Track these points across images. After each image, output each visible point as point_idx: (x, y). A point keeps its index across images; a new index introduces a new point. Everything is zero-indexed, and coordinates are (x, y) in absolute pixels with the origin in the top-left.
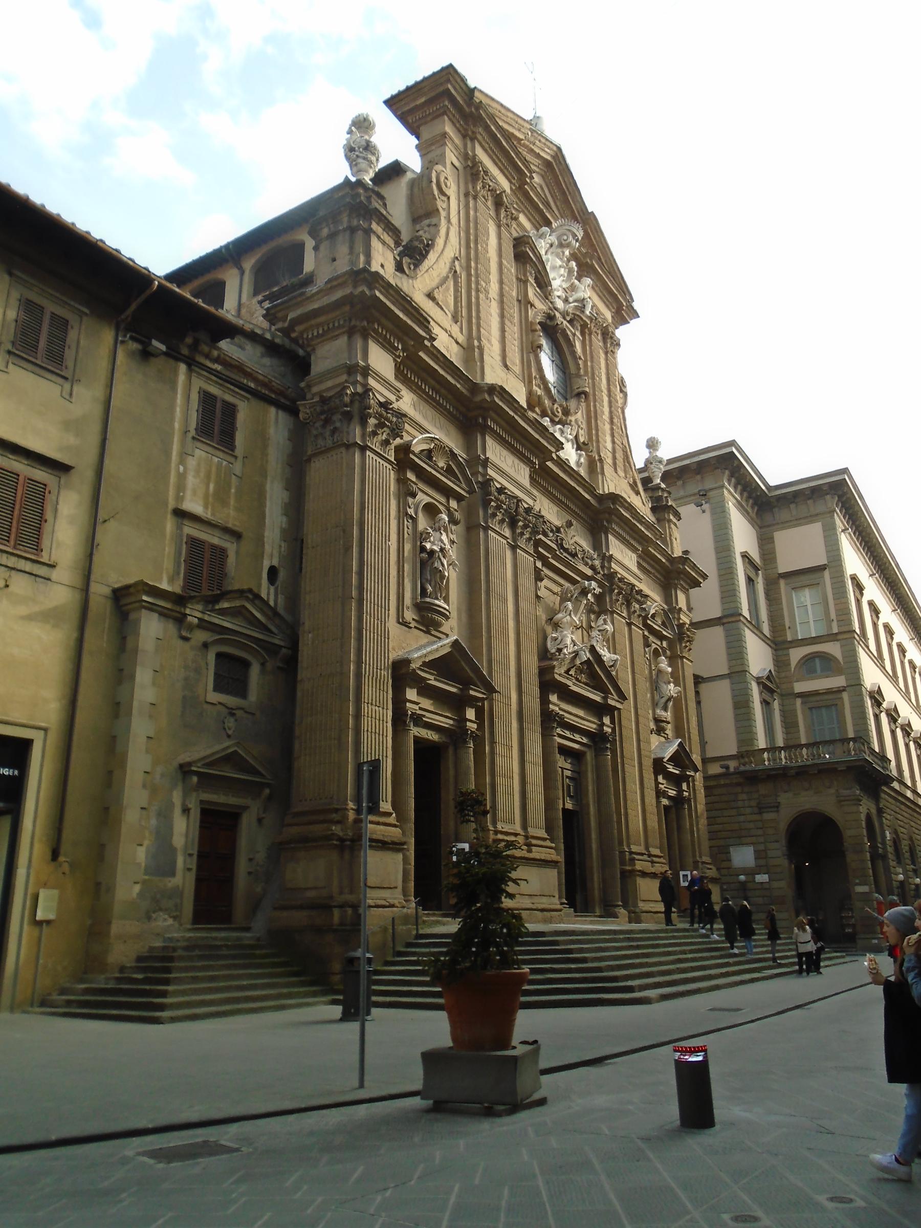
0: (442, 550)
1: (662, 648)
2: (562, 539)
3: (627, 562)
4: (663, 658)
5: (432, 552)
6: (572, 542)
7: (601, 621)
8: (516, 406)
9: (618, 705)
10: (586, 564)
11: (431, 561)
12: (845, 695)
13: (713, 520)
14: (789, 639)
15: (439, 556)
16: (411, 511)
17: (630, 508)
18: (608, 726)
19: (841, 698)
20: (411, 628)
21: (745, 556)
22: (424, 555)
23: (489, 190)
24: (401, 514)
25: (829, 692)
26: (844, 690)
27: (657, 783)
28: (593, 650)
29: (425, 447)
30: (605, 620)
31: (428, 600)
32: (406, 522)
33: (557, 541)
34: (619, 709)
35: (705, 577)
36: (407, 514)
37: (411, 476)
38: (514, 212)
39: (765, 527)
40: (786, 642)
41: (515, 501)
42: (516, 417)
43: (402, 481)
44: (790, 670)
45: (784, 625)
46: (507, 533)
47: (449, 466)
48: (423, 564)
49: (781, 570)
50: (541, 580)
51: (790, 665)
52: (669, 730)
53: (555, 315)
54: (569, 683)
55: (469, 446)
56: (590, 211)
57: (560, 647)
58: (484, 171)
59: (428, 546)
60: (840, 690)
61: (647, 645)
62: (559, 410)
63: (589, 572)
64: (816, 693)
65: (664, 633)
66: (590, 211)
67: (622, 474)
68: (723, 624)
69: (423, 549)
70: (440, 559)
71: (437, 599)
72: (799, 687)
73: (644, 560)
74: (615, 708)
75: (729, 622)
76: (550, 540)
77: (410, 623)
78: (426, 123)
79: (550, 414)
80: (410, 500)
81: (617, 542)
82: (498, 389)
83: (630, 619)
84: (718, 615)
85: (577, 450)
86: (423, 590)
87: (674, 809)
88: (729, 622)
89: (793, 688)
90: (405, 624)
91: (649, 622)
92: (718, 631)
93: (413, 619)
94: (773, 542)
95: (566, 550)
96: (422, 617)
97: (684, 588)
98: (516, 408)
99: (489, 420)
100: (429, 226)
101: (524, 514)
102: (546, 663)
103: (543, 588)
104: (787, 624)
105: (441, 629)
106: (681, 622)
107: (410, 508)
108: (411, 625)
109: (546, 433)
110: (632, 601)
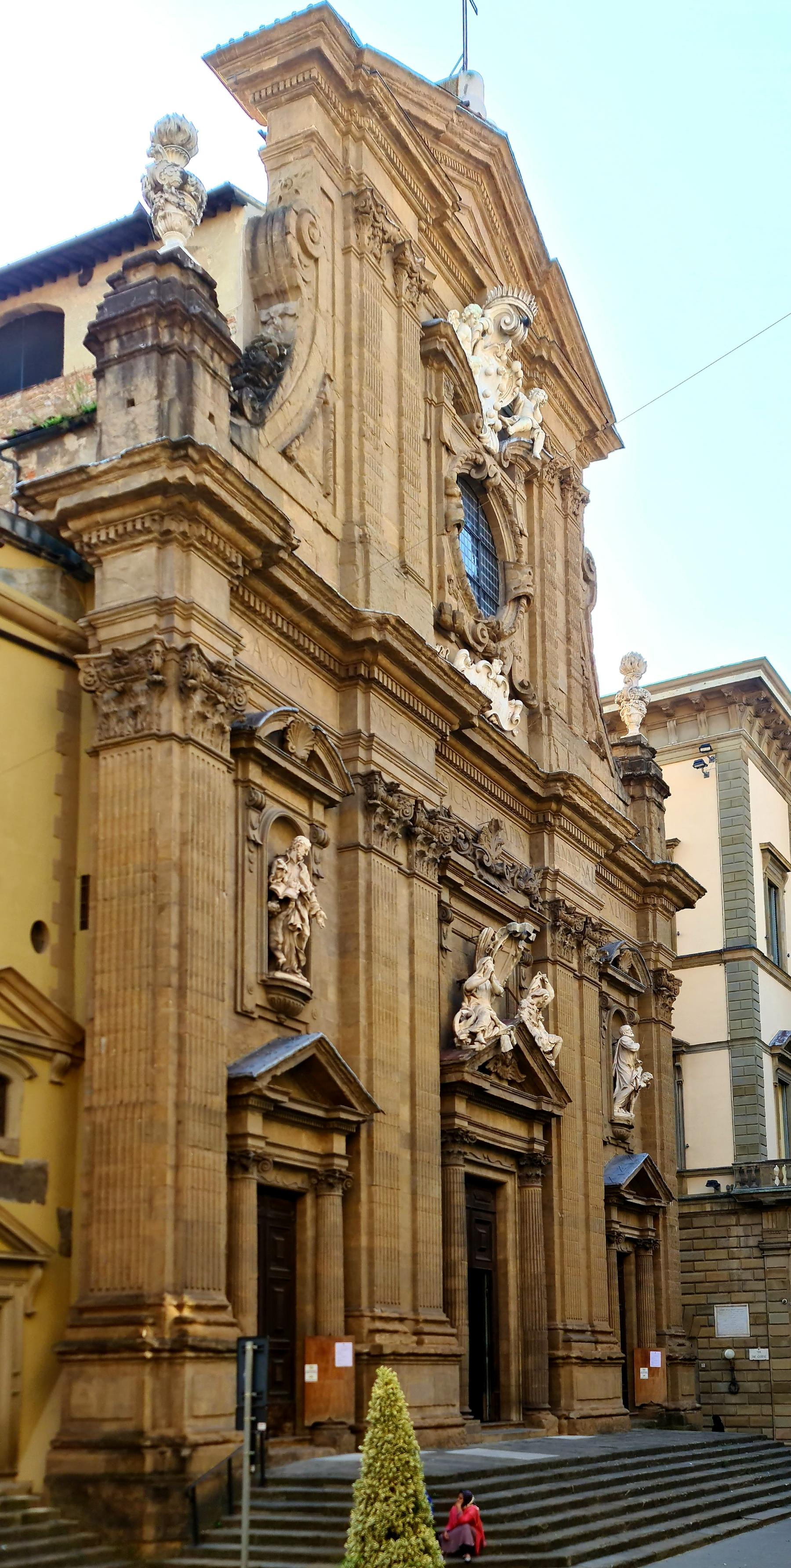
0: (301, 894)
1: (628, 1008)
2: (483, 852)
3: (580, 880)
4: (628, 1027)
5: (286, 901)
6: (495, 854)
7: (536, 982)
8: (420, 646)
9: (556, 1112)
10: (518, 889)
11: (285, 913)
13: (720, 790)
15: (296, 905)
16: (255, 835)
17: (590, 793)
18: (540, 1144)
20: (253, 1019)
21: (768, 851)
22: (274, 905)
23: (384, 241)
24: (240, 838)
27: (609, 1221)
28: (522, 1029)
29: (277, 726)
30: (543, 981)
31: (279, 975)
32: (247, 852)
33: (474, 855)
34: (558, 1117)
35: (701, 892)
36: (249, 840)
37: (255, 773)
38: (423, 277)
41: (413, 802)
42: (420, 665)
43: (243, 783)
46: (401, 855)
47: (313, 755)
48: (272, 916)
50: (449, 922)
52: (635, 1141)
53: (484, 462)
54: (486, 1085)
55: (346, 711)
57: (474, 1030)
58: (377, 205)
59: (281, 890)
61: (604, 1007)
62: (486, 634)
63: (522, 901)
65: (633, 986)
67: (578, 729)
68: (725, 962)
69: (272, 895)
70: (299, 911)
71: (293, 972)
73: (607, 868)
74: (551, 1115)
75: (734, 960)
76: (464, 856)
77: (252, 1013)
78: (278, 105)
79: (472, 641)
80: (254, 815)
81: (567, 847)
82: (393, 621)
83: (580, 970)
84: (719, 947)
85: (511, 698)
86: (272, 959)
87: (633, 1256)
88: (734, 960)
90: (245, 1014)
91: (610, 971)
92: (716, 973)
93: (257, 1006)
95: (488, 870)
96: (271, 1001)
97: (668, 910)
98: (420, 650)
99: (376, 669)
100: (283, 315)
101: (426, 823)
102: (451, 1057)
103: (450, 935)
105: (298, 1018)
106: (660, 966)
107: (253, 828)
108: (255, 1015)
109: (466, 687)
110: (585, 942)
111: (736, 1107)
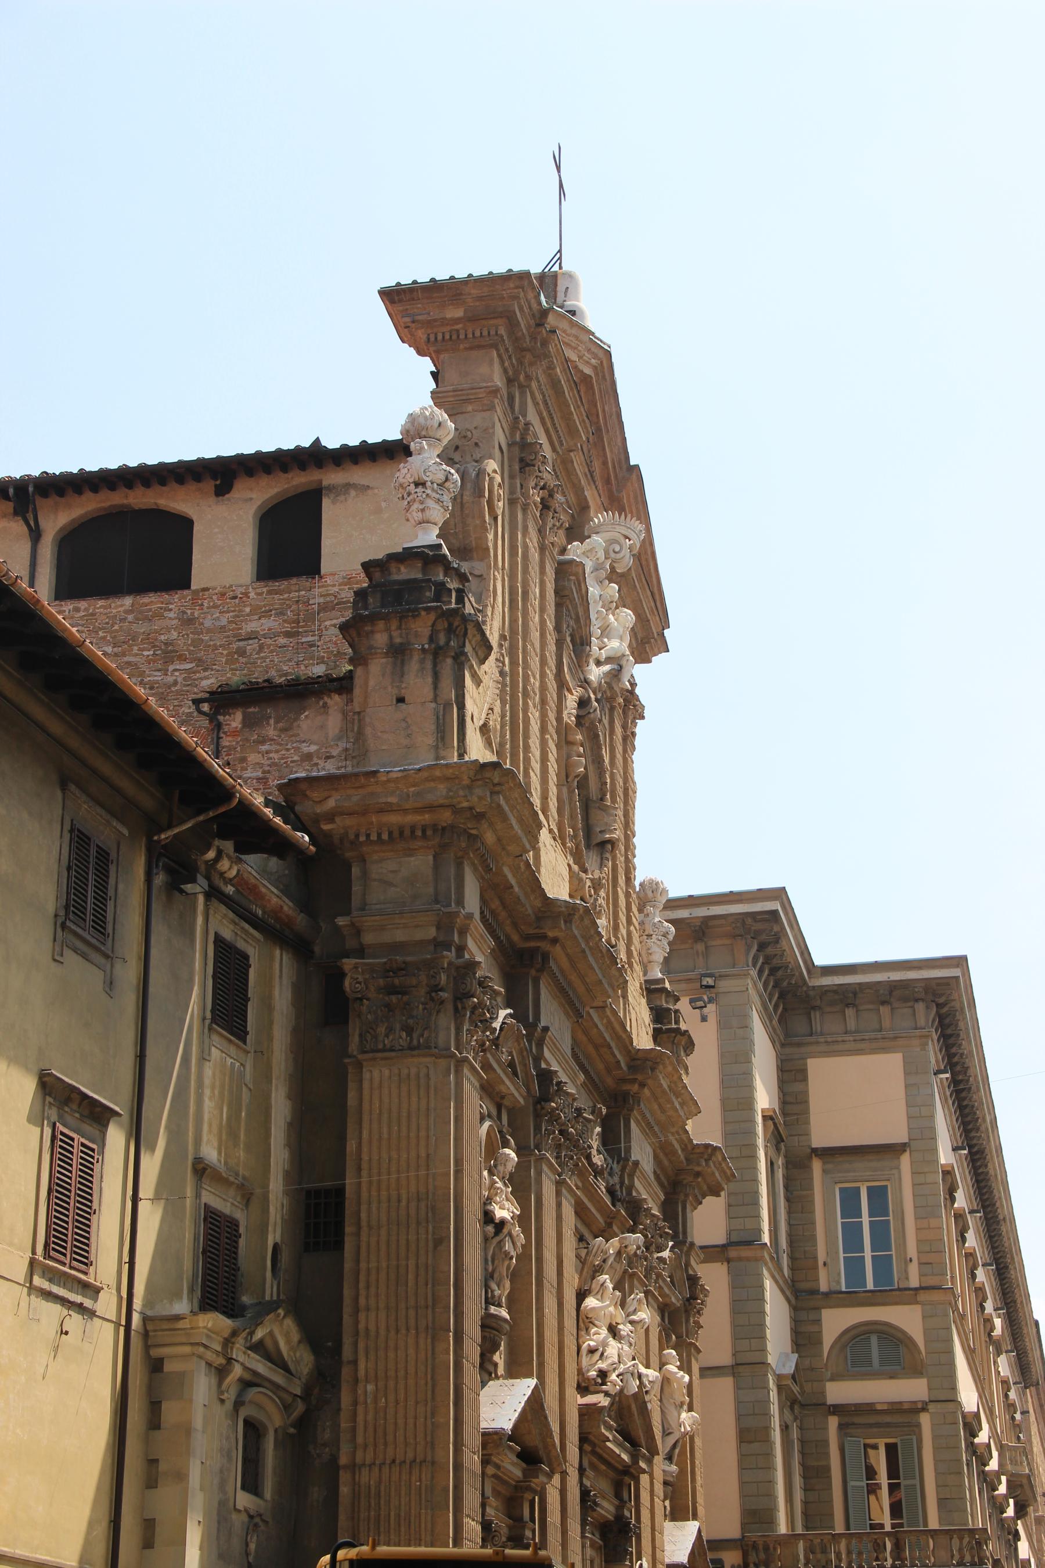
12: (925, 1419)
14: (824, 1287)
19: (918, 1425)
25: (896, 1408)
26: (924, 1409)
39: (791, 1045)
40: (814, 1292)
44: (821, 1355)
45: (815, 1258)
49: (819, 1140)
51: (820, 1342)
56: (632, 463)
60: (917, 1409)
64: (868, 1409)
66: (632, 463)
72: (838, 1392)
89: (823, 1393)
94: (805, 1079)
104: (821, 1256)
111: (742, 1457)
